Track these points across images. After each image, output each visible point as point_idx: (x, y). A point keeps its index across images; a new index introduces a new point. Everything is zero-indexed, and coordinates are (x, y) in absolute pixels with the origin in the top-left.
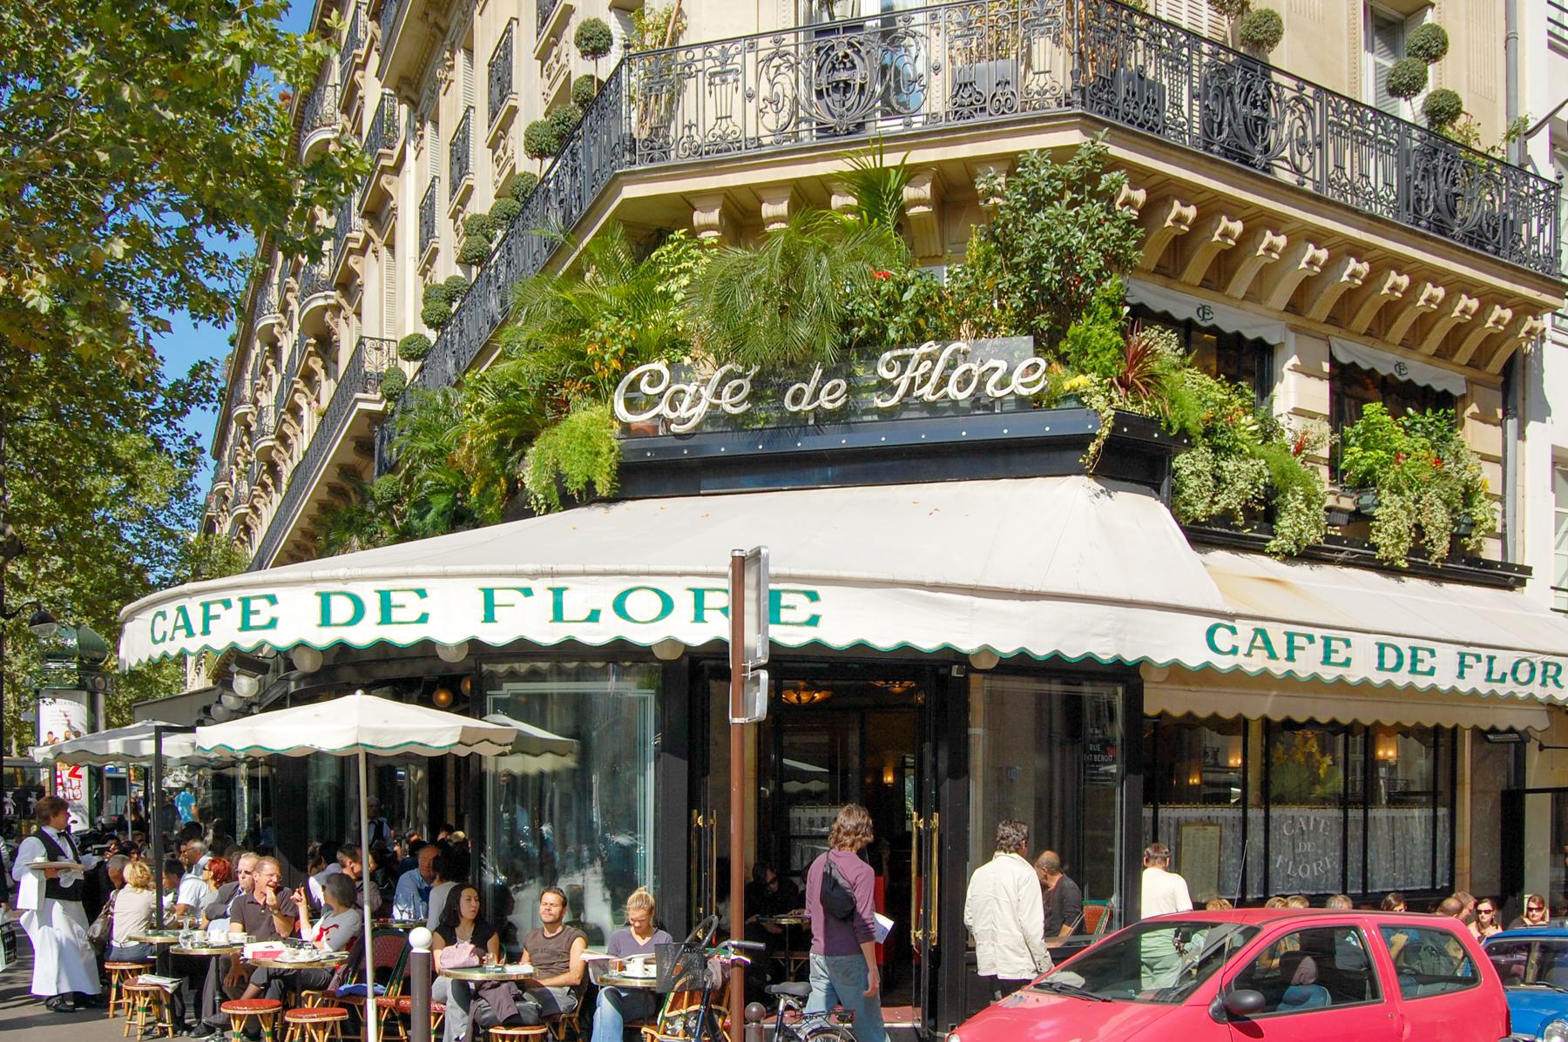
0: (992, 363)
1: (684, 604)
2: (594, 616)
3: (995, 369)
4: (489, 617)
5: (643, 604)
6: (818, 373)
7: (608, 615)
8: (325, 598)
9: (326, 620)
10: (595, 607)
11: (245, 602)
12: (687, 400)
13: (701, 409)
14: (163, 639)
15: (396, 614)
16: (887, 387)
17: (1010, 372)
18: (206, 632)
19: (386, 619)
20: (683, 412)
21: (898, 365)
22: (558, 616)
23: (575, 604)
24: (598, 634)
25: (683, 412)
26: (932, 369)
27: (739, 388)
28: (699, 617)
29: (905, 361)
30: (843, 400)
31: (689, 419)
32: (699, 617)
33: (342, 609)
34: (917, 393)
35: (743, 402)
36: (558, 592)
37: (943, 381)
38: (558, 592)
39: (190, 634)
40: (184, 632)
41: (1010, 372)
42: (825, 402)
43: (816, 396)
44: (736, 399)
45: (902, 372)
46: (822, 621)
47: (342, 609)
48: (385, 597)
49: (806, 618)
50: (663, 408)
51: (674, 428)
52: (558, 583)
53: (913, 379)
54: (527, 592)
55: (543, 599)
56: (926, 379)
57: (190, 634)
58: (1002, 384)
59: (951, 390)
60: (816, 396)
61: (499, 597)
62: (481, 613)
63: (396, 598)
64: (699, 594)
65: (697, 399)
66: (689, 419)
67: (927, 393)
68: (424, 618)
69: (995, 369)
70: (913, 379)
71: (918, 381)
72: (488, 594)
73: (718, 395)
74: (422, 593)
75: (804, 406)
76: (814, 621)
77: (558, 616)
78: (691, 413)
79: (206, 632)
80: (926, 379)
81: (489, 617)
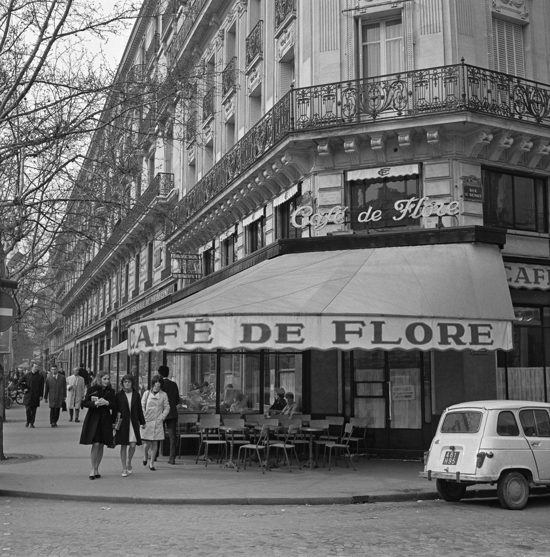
6: (370, 209)
16: (399, 214)
21: (402, 205)
26: (415, 207)
29: (405, 204)
30: (380, 218)
43: (370, 216)
45: (404, 208)
56: (413, 210)
60: (370, 216)
70: (408, 211)
75: (365, 220)
80: (413, 210)
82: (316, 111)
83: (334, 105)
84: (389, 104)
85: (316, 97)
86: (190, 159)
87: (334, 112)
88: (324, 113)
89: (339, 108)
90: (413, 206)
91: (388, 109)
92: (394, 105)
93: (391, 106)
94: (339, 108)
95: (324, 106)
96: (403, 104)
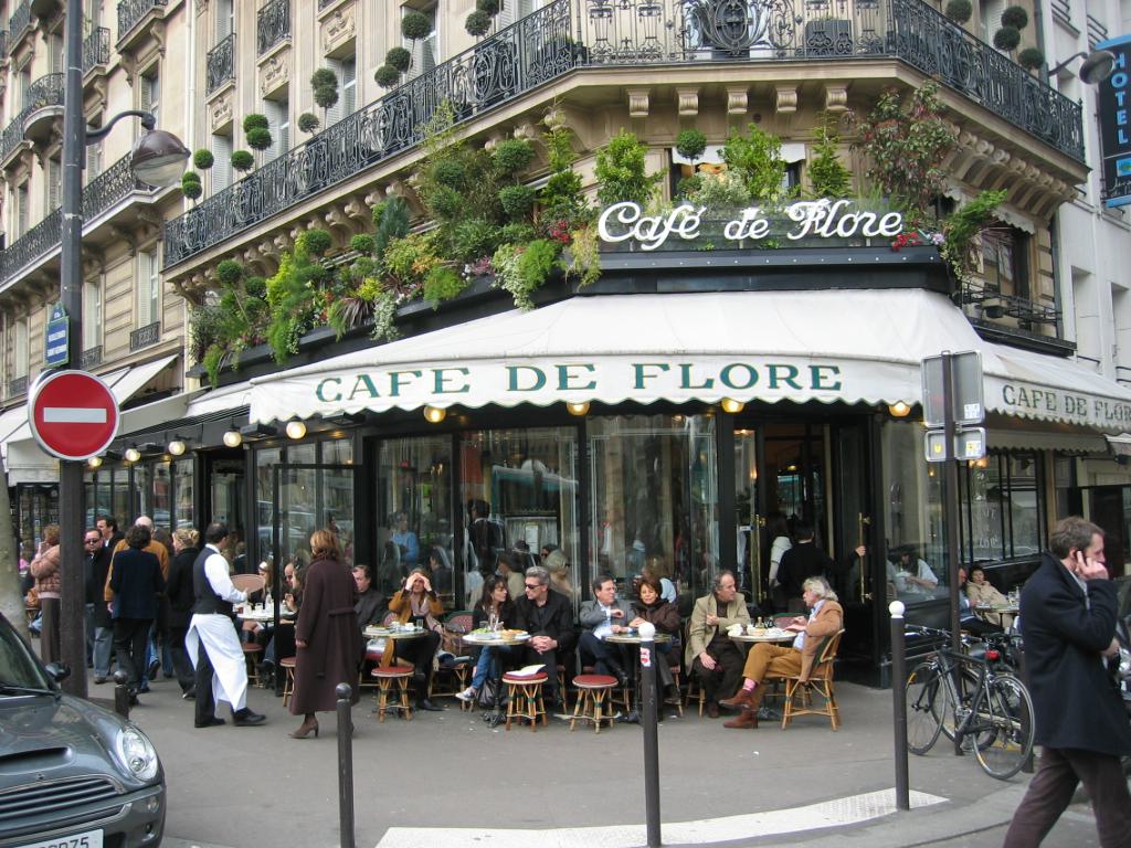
0: (866, 215)
1: (764, 375)
2: (709, 384)
3: (867, 219)
4: (639, 385)
5: (739, 376)
7: (718, 383)
8: (513, 371)
9: (513, 386)
10: (711, 377)
11: (438, 373)
12: (654, 228)
13: (663, 236)
14: (339, 397)
15: (570, 382)
17: (878, 221)
18: (395, 392)
19: (563, 385)
20: (650, 235)
22: (686, 384)
23: (697, 377)
24: (712, 396)
25: (650, 235)
27: (691, 223)
28: (773, 385)
31: (656, 241)
32: (773, 385)
33: (526, 378)
34: (817, 231)
35: (693, 232)
36: (685, 368)
37: (835, 223)
38: (685, 368)
39: (374, 393)
40: (368, 393)
41: (878, 221)
42: (753, 234)
44: (688, 230)
46: (842, 386)
47: (526, 378)
48: (563, 371)
49: (832, 385)
50: (635, 232)
51: (645, 247)
52: (686, 361)
53: (814, 222)
54: (665, 367)
55: (676, 372)
56: (822, 222)
57: (374, 393)
58: (873, 229)
59: (840, 230)
61: (646, 371)
62: (634, 382)
63: (570, 371)
64: (773, 369)
65: (661, 228)
66: (656, 241)
67: (823, 231)
68: (592, 385)
69: (867, 219)
71: (817, 224)
72: (639, 368)
73: (676, 225)
74: (591, 368)
75: (738, 236)
76: (837, 386)
77: (686, 384)
78: (655, 238)
79: (395, 392)
80: (822, 222)
81: (639, 385)
82: (627, 34)
83: (661, 25)
84: (762, 35)
85: (625, 8)
86: (217, 122)
87: (661, 39)
88: (641, 38)
89: (670, 33)
90: (822, 215)
91: (760, 43)
92: (771, 37)
93: (765, 38)
94: (670, 33)
95: (640, 26)
96: (786, 38)
